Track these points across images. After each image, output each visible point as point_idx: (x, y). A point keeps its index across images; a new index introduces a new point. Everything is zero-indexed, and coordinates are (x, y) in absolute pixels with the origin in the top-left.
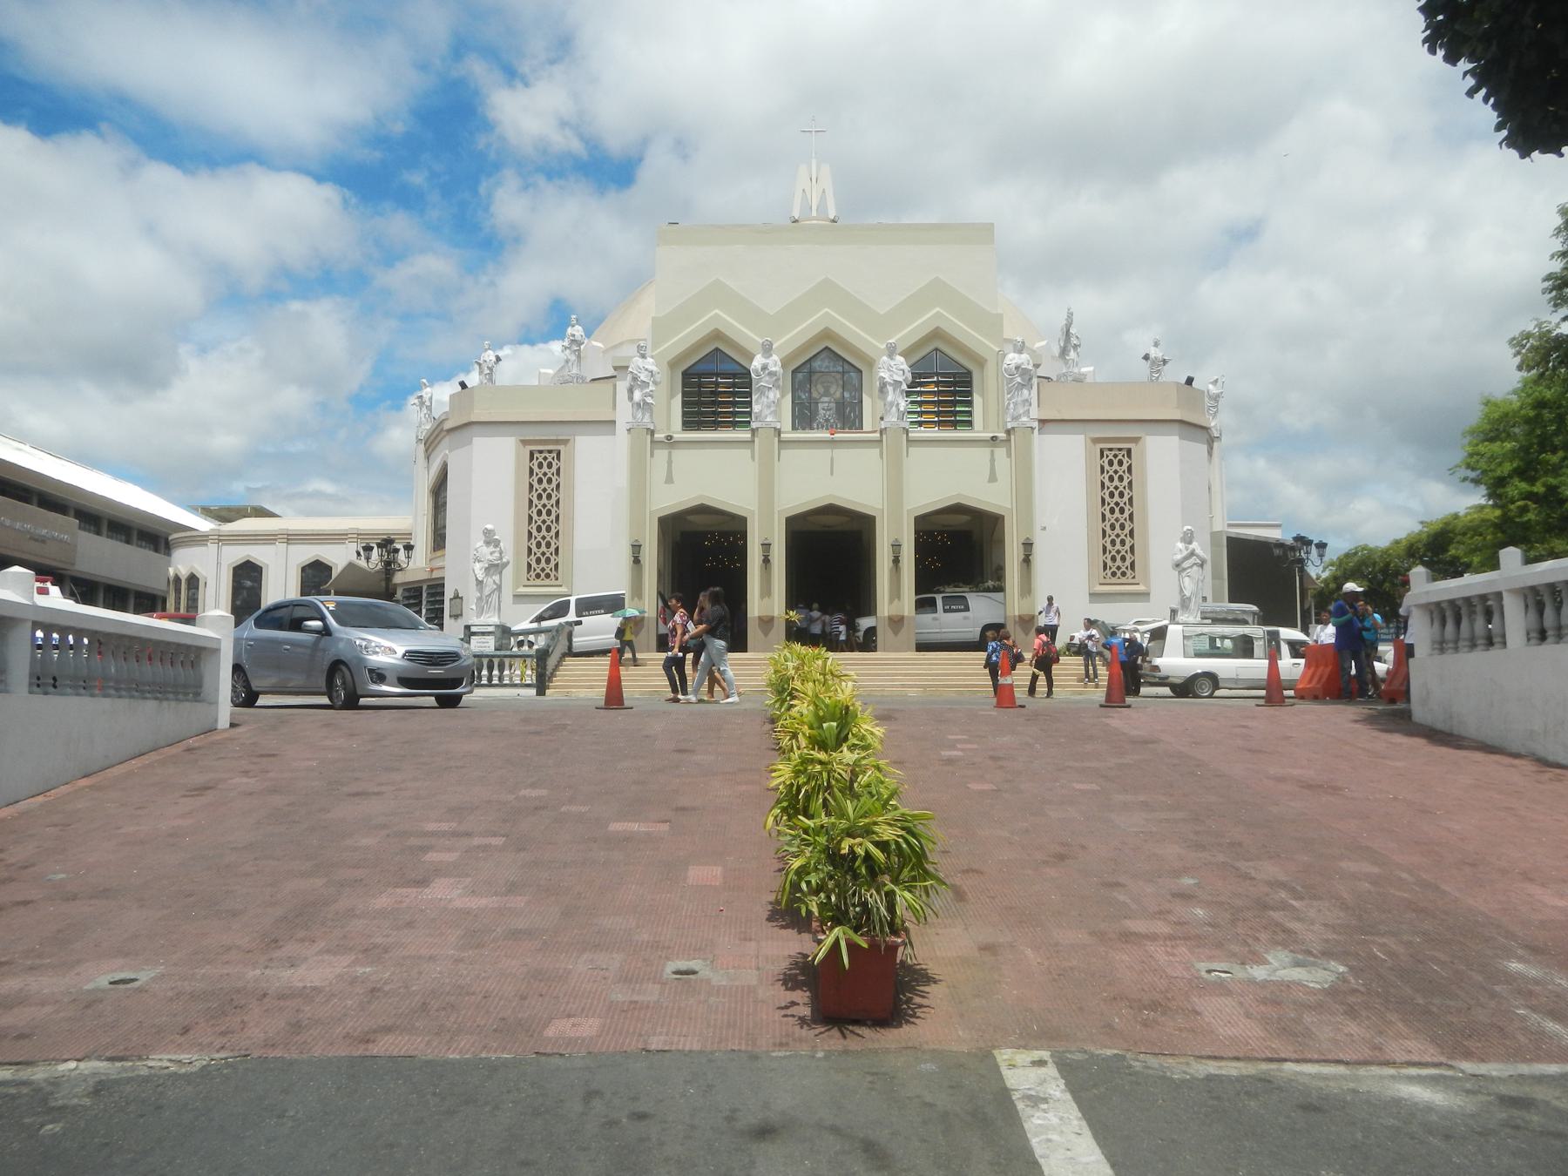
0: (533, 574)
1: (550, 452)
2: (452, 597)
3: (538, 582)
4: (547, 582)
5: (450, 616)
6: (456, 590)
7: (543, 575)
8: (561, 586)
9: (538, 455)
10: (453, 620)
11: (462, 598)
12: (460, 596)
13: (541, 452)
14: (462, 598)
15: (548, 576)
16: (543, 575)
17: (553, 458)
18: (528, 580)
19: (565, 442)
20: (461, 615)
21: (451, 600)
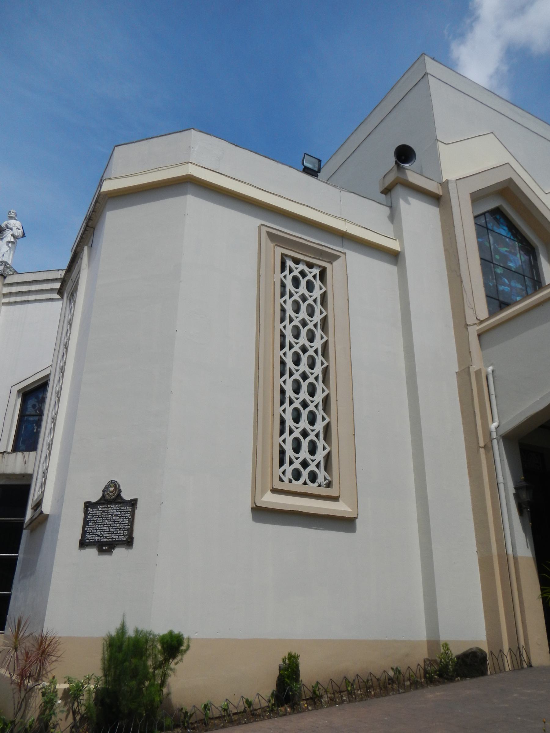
0: (289, 470)
1: (311, 266)
2: (94, 500)
3: (297, 486)
4: (312, 488)
5: (83, 544)
6: (114, 484)
7: (305, 474)
8: (335, 499)
9: (293, 265)
10: (92, 552)
11: (133, 503)
12: (126, 496)
13: (297, 261)
14: (133, 503)
15: (313, 477)
16: (305, 474)
17: (314, 277)
18: (281, 480)
19: (332, 258)
20: (129, 542)
21: (88, 505)
